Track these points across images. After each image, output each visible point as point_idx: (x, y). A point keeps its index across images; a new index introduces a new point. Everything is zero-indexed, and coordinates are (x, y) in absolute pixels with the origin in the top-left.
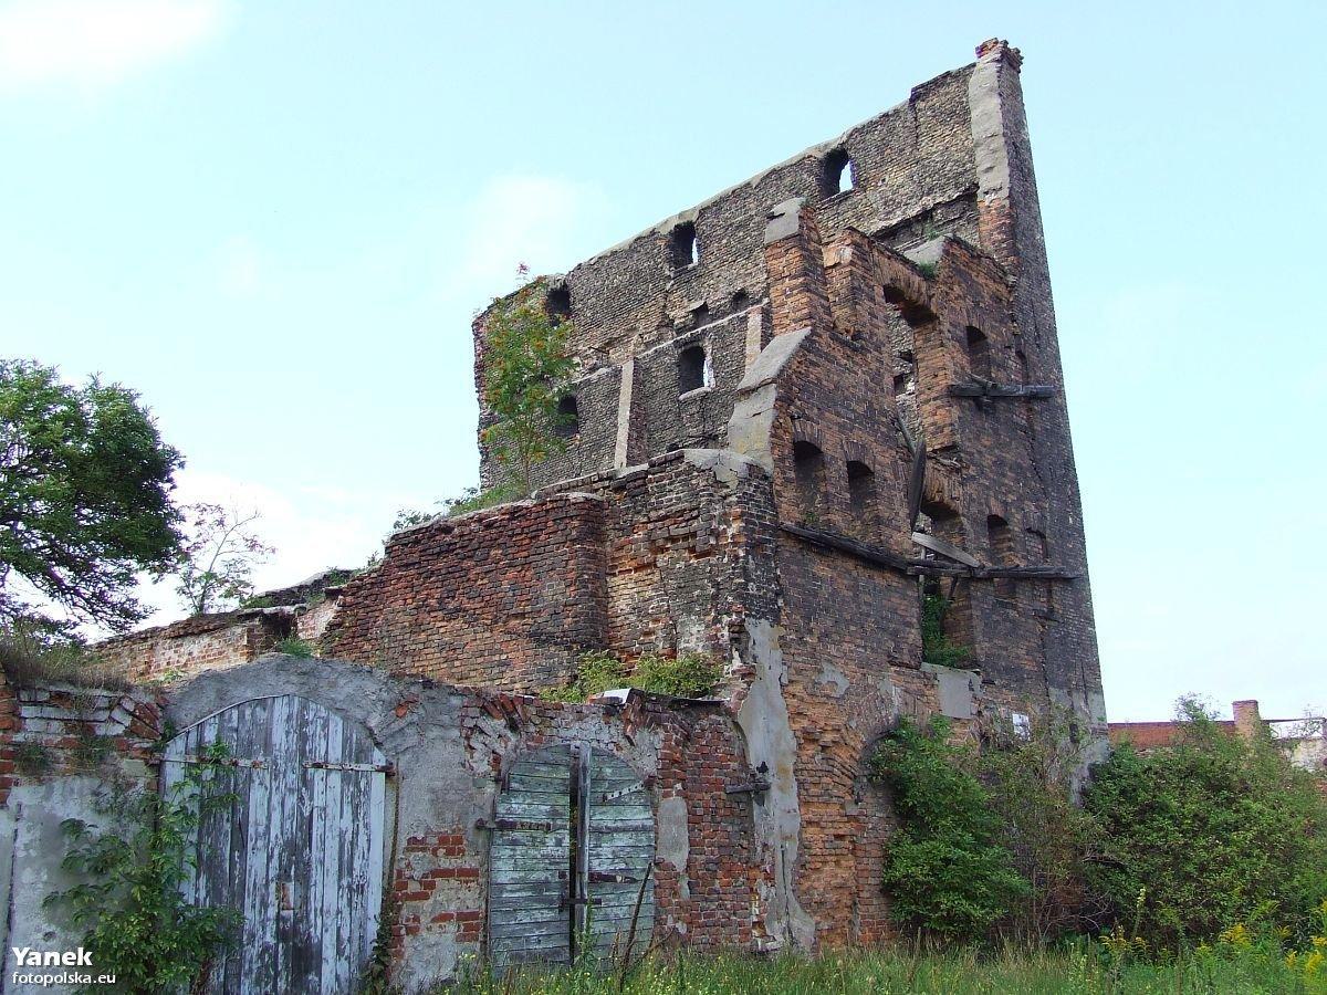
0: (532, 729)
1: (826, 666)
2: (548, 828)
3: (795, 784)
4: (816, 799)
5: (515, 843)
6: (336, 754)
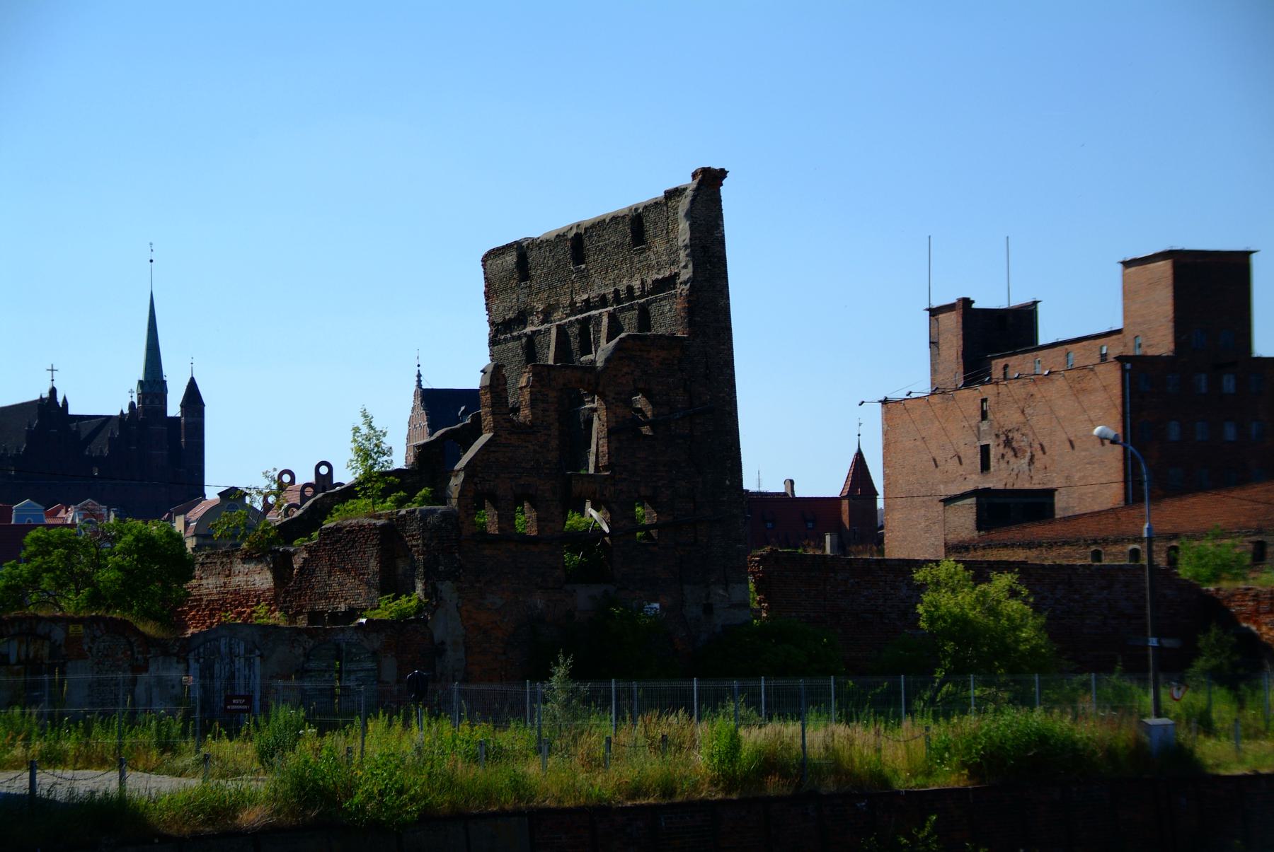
0: (321, 638)
2: (326, 671)
5: (311, 677)
6: (242, 652)
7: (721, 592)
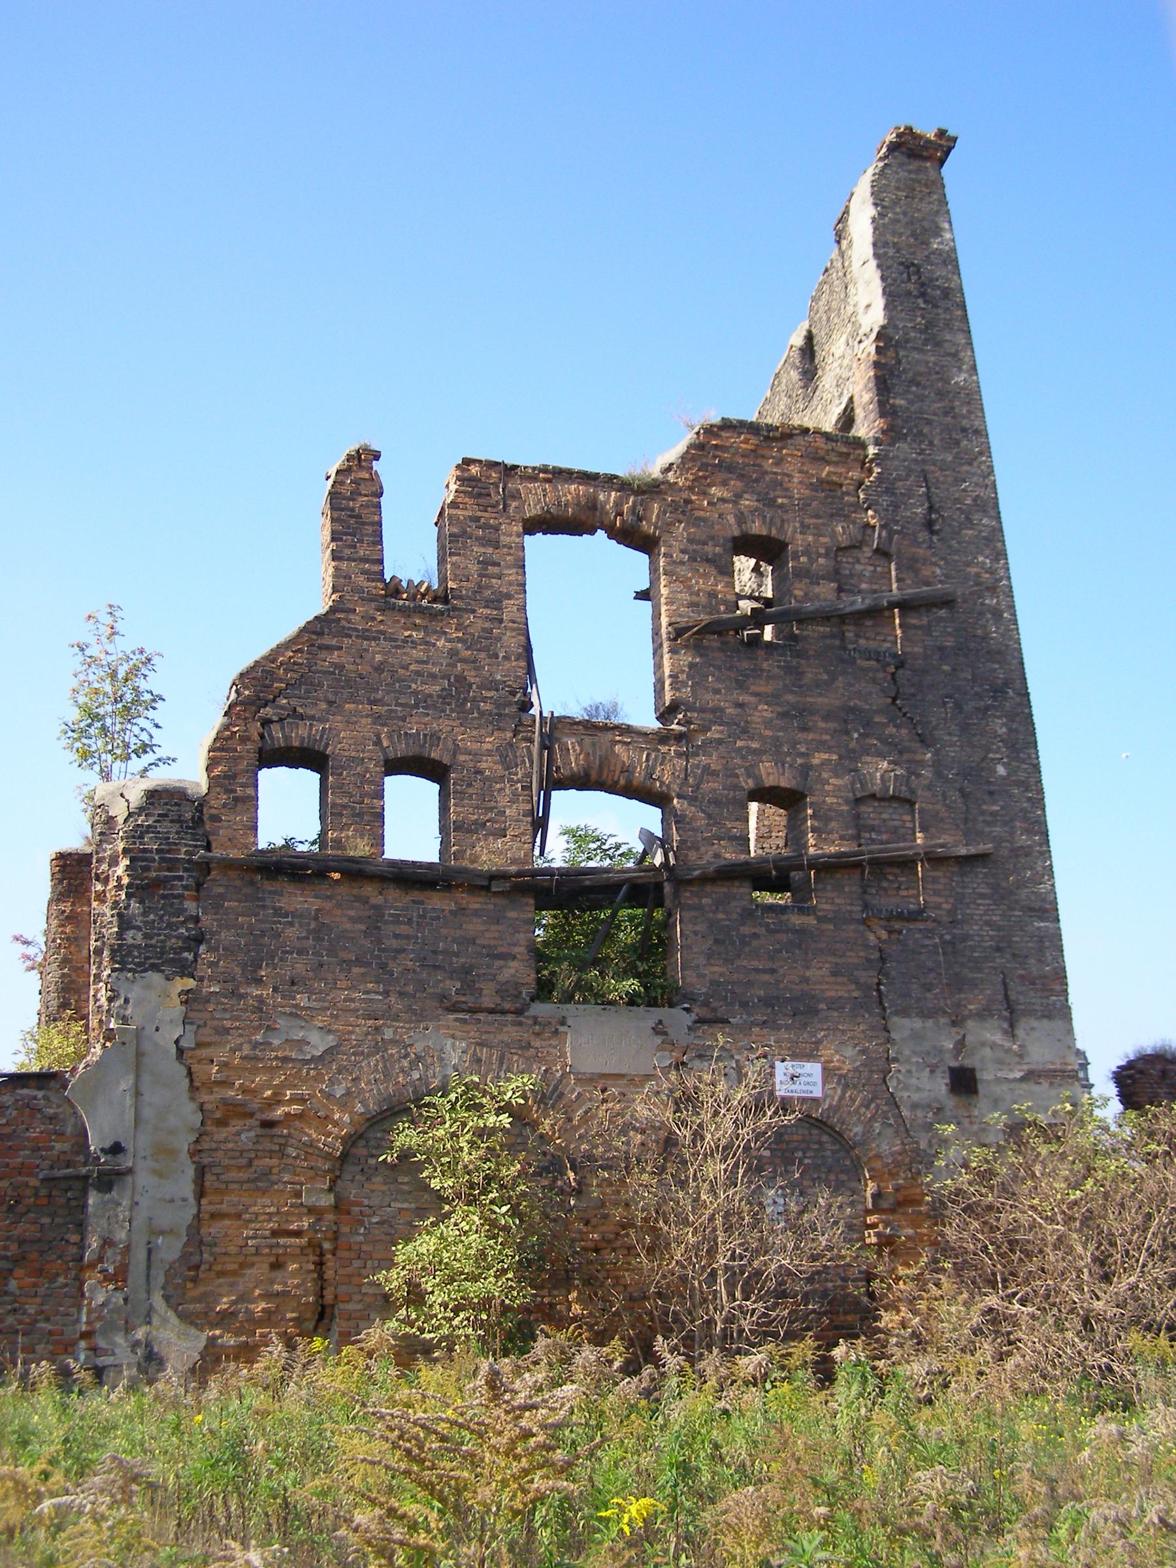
1: (281, 1022)
3: (190, 1172)
4: (235, 1186)
7: (998, 1038)
